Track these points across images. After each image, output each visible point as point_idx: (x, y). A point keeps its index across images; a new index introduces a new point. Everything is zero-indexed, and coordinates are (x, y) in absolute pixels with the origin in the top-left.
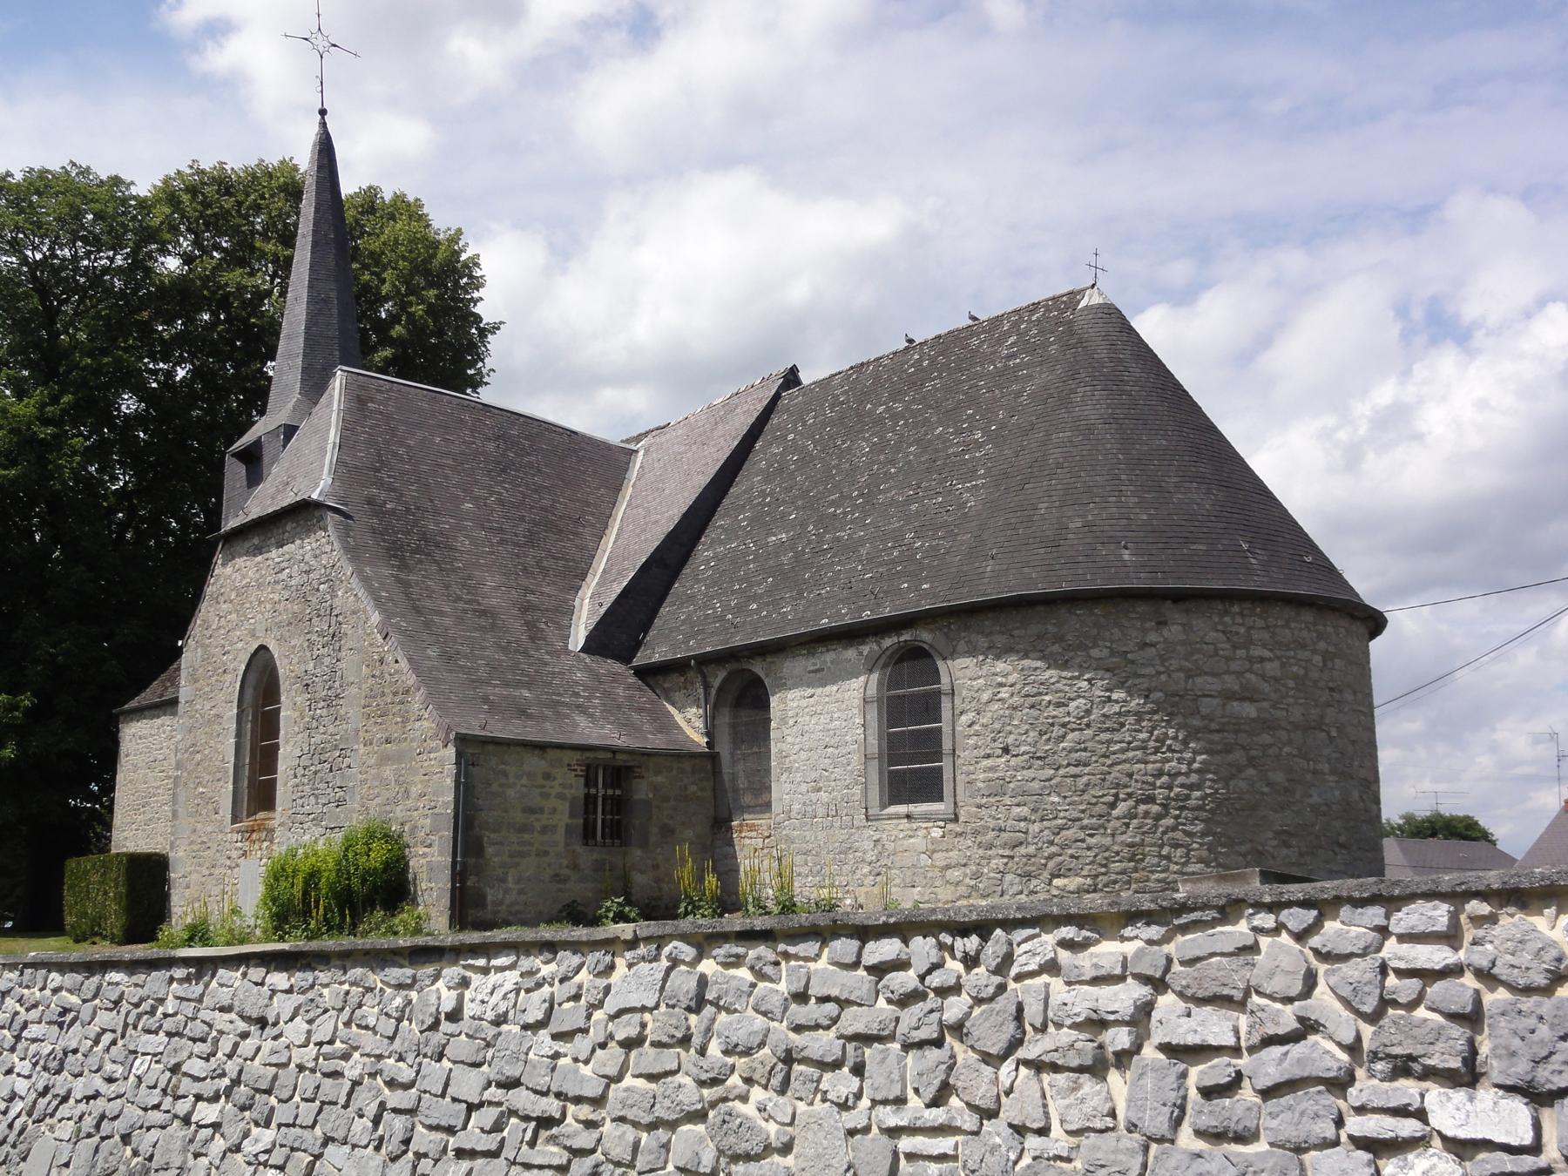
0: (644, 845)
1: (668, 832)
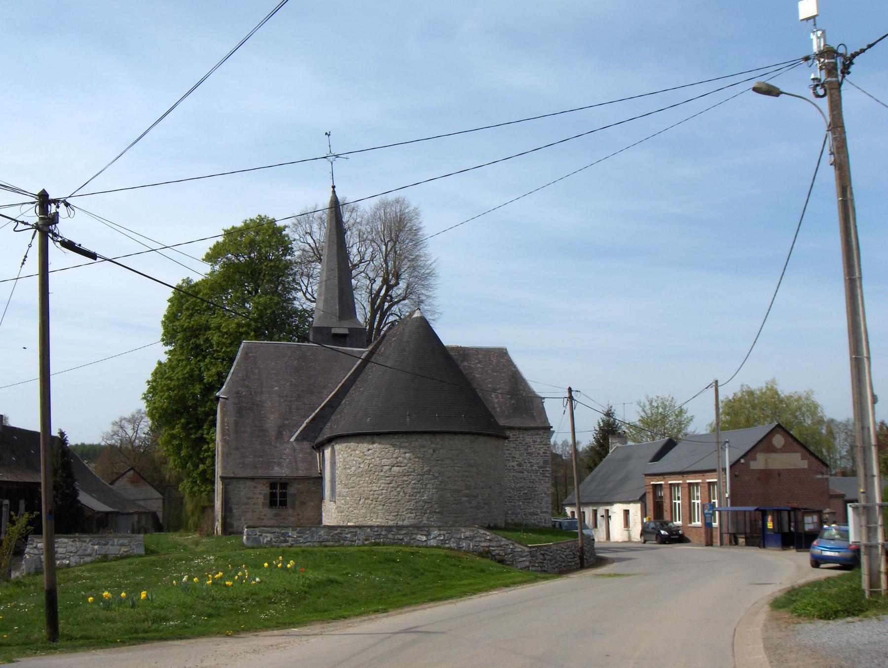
0: (293, 507)
1: (303, 503)
